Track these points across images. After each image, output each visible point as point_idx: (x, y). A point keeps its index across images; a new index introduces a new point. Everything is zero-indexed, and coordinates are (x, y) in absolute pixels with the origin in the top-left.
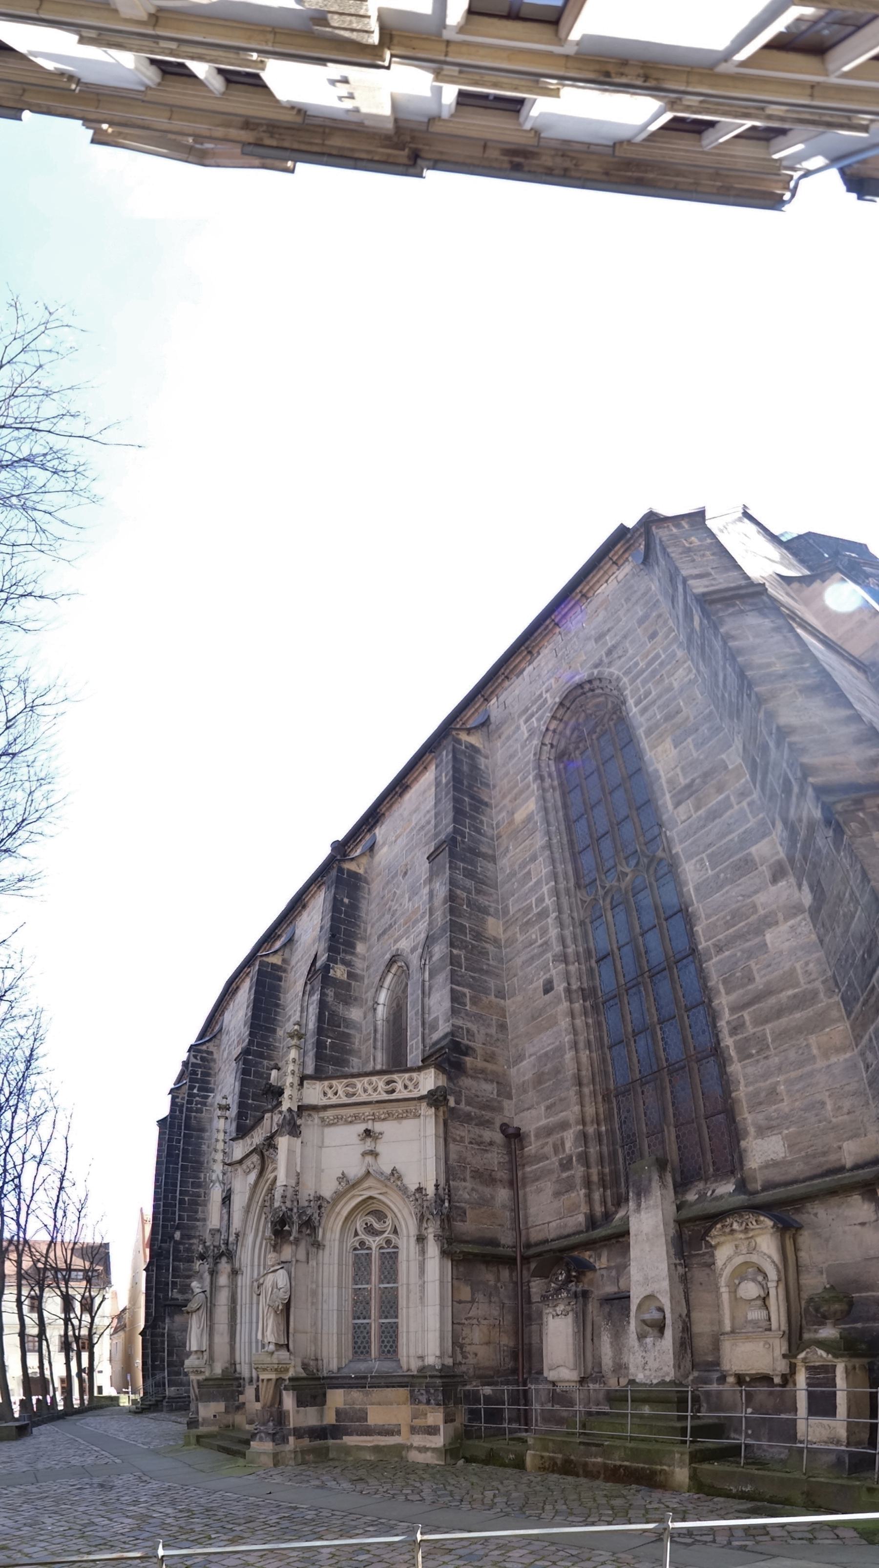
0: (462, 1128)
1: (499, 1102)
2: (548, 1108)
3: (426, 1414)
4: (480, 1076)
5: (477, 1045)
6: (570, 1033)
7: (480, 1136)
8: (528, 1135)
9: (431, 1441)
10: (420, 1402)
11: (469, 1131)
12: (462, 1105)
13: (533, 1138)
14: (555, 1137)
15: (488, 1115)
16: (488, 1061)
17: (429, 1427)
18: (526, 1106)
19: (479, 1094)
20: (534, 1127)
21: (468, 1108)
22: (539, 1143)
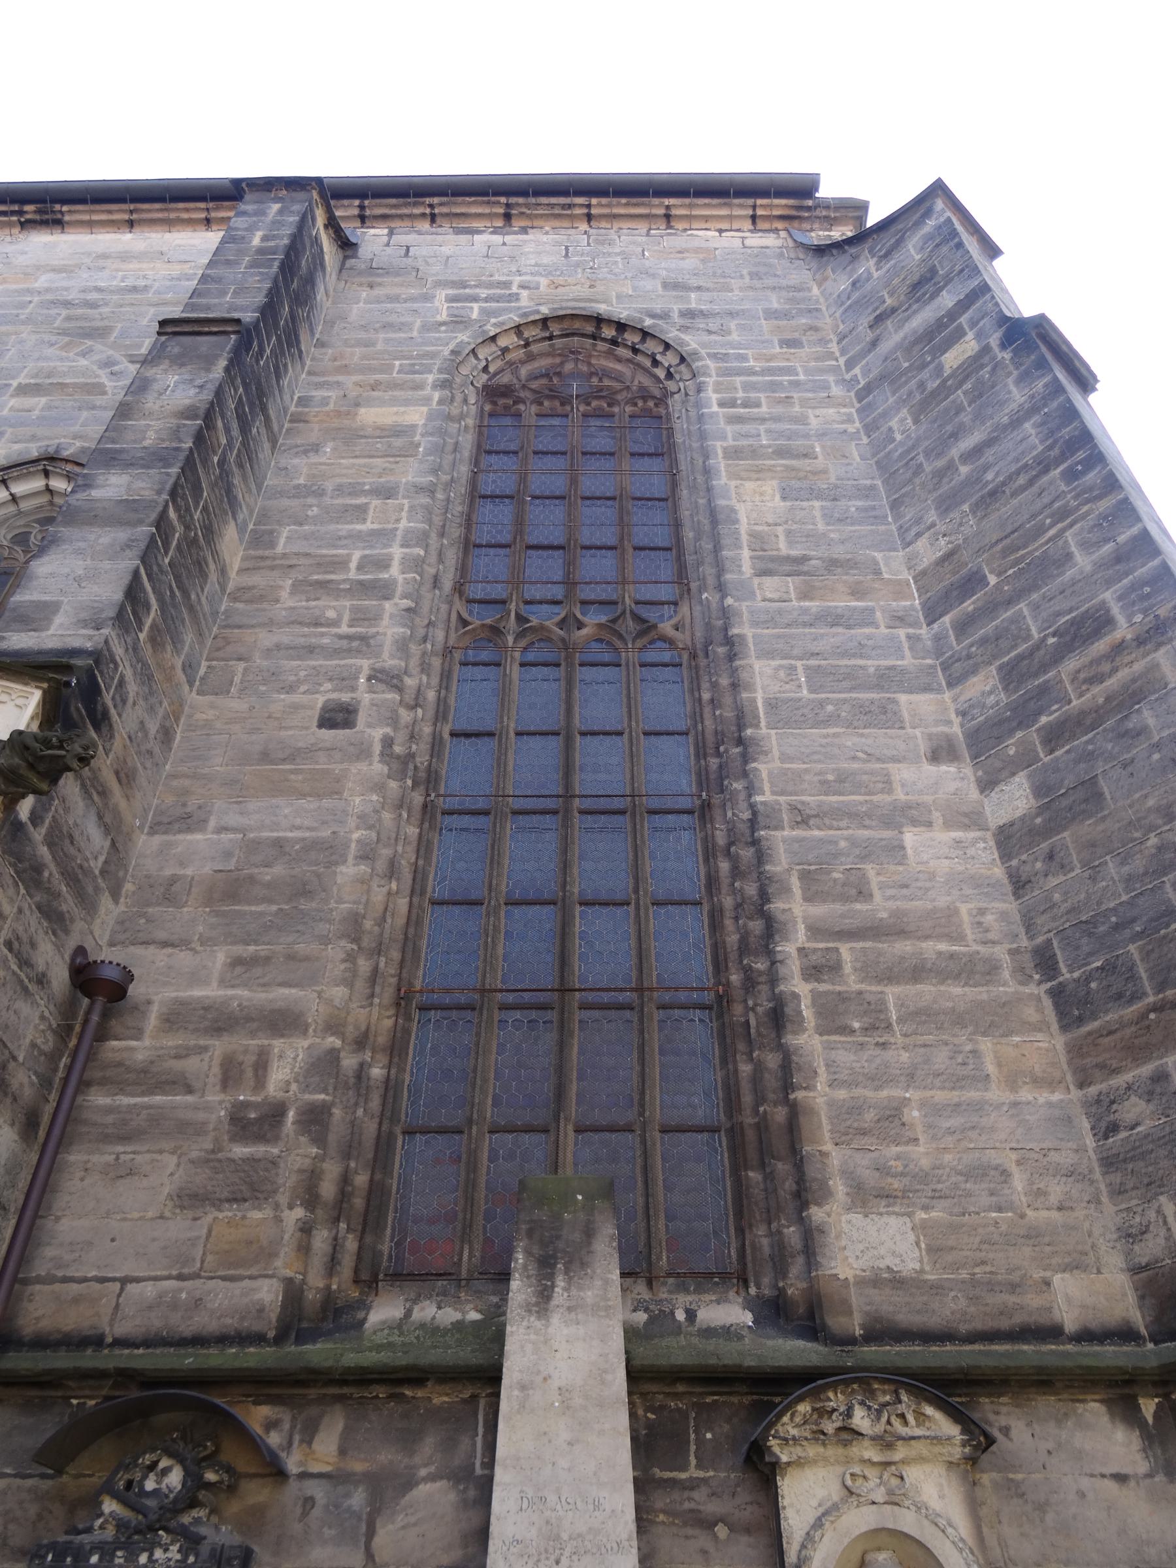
0: (11, 891)
1: (97, 889)
2: (237, 962)
4: (96, 797)
5: (125, 722)
7: (33, 945)
8: (138, 1011)
11: (20, 911)
12: (38, 835)
13: (152, 1020)
14: (244, 1043)
15: (68, 904)
16: (120, 781)
18: (162, 935)
19: (76, 835)
20: (170, 994)
21: (44, 851)
22: (173, 1041)
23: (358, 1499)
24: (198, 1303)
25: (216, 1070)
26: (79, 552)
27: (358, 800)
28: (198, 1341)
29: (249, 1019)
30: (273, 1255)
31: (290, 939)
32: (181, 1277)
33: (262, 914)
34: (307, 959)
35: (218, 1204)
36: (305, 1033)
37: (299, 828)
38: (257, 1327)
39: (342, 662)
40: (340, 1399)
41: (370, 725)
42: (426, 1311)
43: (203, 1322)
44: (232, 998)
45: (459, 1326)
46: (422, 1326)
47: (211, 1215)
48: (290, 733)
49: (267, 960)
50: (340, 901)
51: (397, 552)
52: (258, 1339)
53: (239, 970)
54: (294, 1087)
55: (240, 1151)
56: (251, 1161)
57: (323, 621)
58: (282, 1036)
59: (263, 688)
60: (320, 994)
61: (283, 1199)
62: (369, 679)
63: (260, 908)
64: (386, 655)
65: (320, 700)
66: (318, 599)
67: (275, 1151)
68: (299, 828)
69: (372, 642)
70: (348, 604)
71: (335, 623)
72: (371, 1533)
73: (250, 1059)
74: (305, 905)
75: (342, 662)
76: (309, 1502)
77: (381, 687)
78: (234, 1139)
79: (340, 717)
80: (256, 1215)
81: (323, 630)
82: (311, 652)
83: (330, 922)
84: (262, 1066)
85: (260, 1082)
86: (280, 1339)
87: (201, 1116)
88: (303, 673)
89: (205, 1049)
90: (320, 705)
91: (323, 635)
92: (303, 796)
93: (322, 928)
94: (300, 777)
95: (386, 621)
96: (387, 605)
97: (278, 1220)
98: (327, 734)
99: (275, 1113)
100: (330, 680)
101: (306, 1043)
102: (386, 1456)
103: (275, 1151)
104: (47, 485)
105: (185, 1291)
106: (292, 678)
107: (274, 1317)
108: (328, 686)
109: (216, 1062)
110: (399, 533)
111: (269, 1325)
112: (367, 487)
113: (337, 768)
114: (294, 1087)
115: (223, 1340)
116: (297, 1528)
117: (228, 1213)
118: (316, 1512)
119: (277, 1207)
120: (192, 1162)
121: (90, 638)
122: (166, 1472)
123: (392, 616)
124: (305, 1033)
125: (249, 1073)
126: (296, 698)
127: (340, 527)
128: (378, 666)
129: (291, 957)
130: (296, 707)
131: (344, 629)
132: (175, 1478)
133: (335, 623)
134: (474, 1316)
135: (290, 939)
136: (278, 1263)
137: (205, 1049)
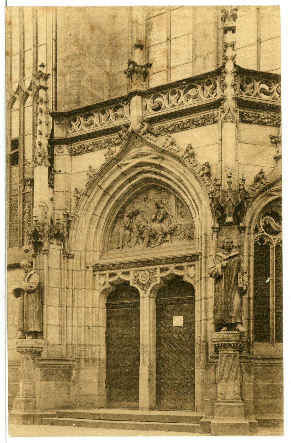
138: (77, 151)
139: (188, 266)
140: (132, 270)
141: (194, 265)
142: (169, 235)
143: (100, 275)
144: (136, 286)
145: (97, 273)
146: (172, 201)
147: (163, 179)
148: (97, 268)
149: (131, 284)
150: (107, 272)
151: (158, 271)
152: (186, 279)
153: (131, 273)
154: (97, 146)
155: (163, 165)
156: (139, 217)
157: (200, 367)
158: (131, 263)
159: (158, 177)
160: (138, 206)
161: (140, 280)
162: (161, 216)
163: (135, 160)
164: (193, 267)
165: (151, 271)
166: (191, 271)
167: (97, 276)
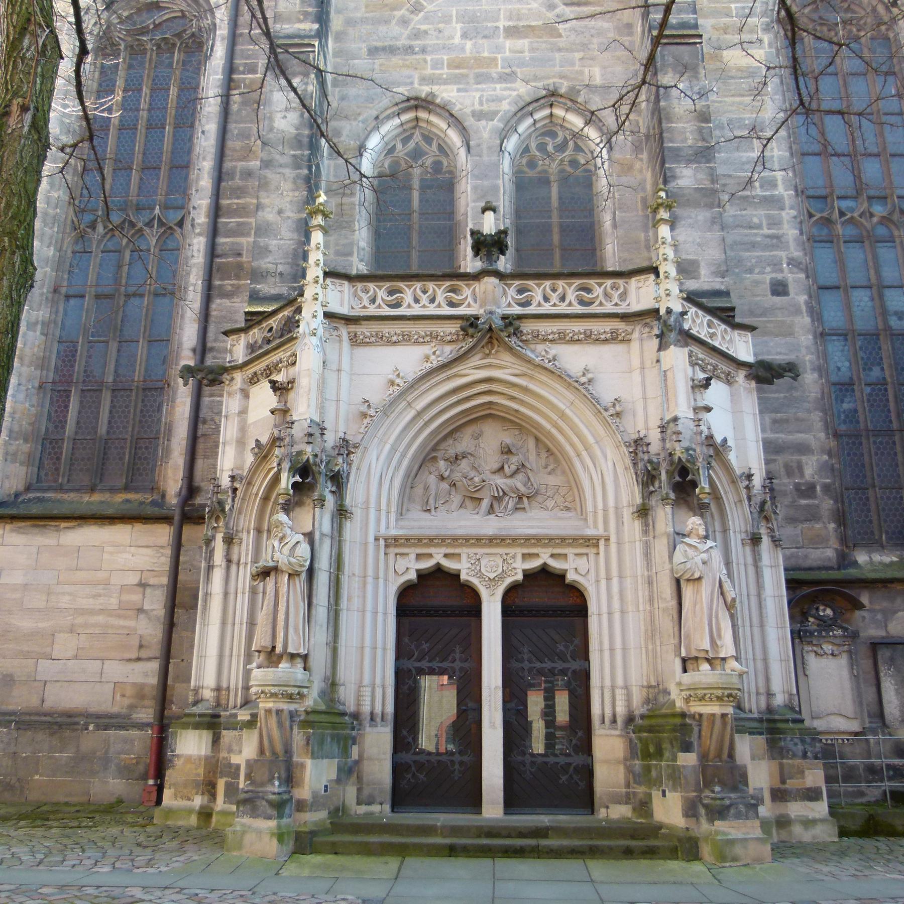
3: (803, 772)
6: (812, 354)
9: (813, 810)
10: (794, 756)
17: (809, 789)
23: (879, 616)
24: (806, 556)
25: (782, 469)
26: (691, 226)
27: (803, 338)
28: (810, 569)
29: (789, 448)
30: (828, 540)
31: (794, 411)
32: (797, 548)
33: (778, 398)
34: (803, 420)
35: (802, 522)
36: (813, 453)
37: (780, 353)
38: (830, 564)
39: (772, 253)
40: (866, 587)
41: (797, 294)
42: (877, 557)
43: (808, 563)
44: (778, 438)
45: (892, 563)
46: (880, 563)
47: (800, 526)
48: (759, 298)
49: (787, 421)
50: (810, 392)
51: (779, 175)
52: (831, 568)
53: (777, 425)
54: (816, 476)
55: (803, 502)
56: (808, 506)
57: (752, 225)
58: (804, 455)
59: (737, 270)
60: (814, 436)
61: (826, 520)
62: (788, 264)
63: (776, 395)
64: (792, 248)
65: (768, 278)
66: (745, 209)
67: (816, 502)
68: (780, 353)
69: (783, 240)
70: (762, 213)
71: (759, 227)
72: (886, 626)
73: (794, 465)
74: (796, 394)
75: (772, 253)
76: (864, 618)
77: (795, 270)
78: (799, 497)
79: (780, 289)
80: (818, 526)
81: (755, 231)
82: (754, 247)
83: (809, 402)
84: (800, 468)
85: (802, 475)
86: (839, 569)
87: (783, 488)
88: (754, 261)
89: (775, 460)
90: (768, 282)
91: (756, 235)
92: (777, 336)
93: (806, 405)
94: (772, 325)
95: (786, 226)
96: (784, 213)
97: (826, 528)
98: (777, 300)
99: (811, 487)
100: (769, 265)
101: (815, 458)
102: (885, 604)
103: (816, 502)
104: (551, 115)
105: (801, 552)
106: (749, 264)
107: (835, 561)
108: (768, 269)
109: (782, 465)
110: (775, 159)
111: (834, 563)
112: (747, 122)
113: (788, 320)
114: (816, 476)
115: (819, 568)
116: (861, 624)
117: (806, 525)
118: (867, 620)
119: (824, 523)
120: (786, 506)
121: (722, 283)
122: (824, 610)
123: (788, 222)
124: (813, 453)
125: (796, 471)
126: (755, 276)
127: (742, 154)
128: (790, 256)
129: (797, 419)
130: (757, 283)
131: (766, 231)
132: (829, 612)
133: (759, 227)
134: (895, 559)
135: (794, 411)
136: (831, 543)
137: (775, 460)
138: (368, 340)
139: (576, 555)
140: (464, 551)
141: (587, 554)
142: (525, 500)
143: (396, 554)
144: (475, 581)
145: (393, 551)
146: (531, 443)
147: (522, 409)
148: (392, 542)
149: (463, 577)
150: (413, 552)
151: (519, 557)
152: (571, 577)
153: (464, 557)
154: (406, 339)
155: (532, 386)
156: (464, 464)
157: (617, 732)
158: (467, 540)
159: (515, 406)
160: (464, 443)
161: (483, 570)
162: (513, 467)
163: (478, 371)
164: (585, 558)
165: (505, 557)
166: (582, 563)
167: (392, 557)
